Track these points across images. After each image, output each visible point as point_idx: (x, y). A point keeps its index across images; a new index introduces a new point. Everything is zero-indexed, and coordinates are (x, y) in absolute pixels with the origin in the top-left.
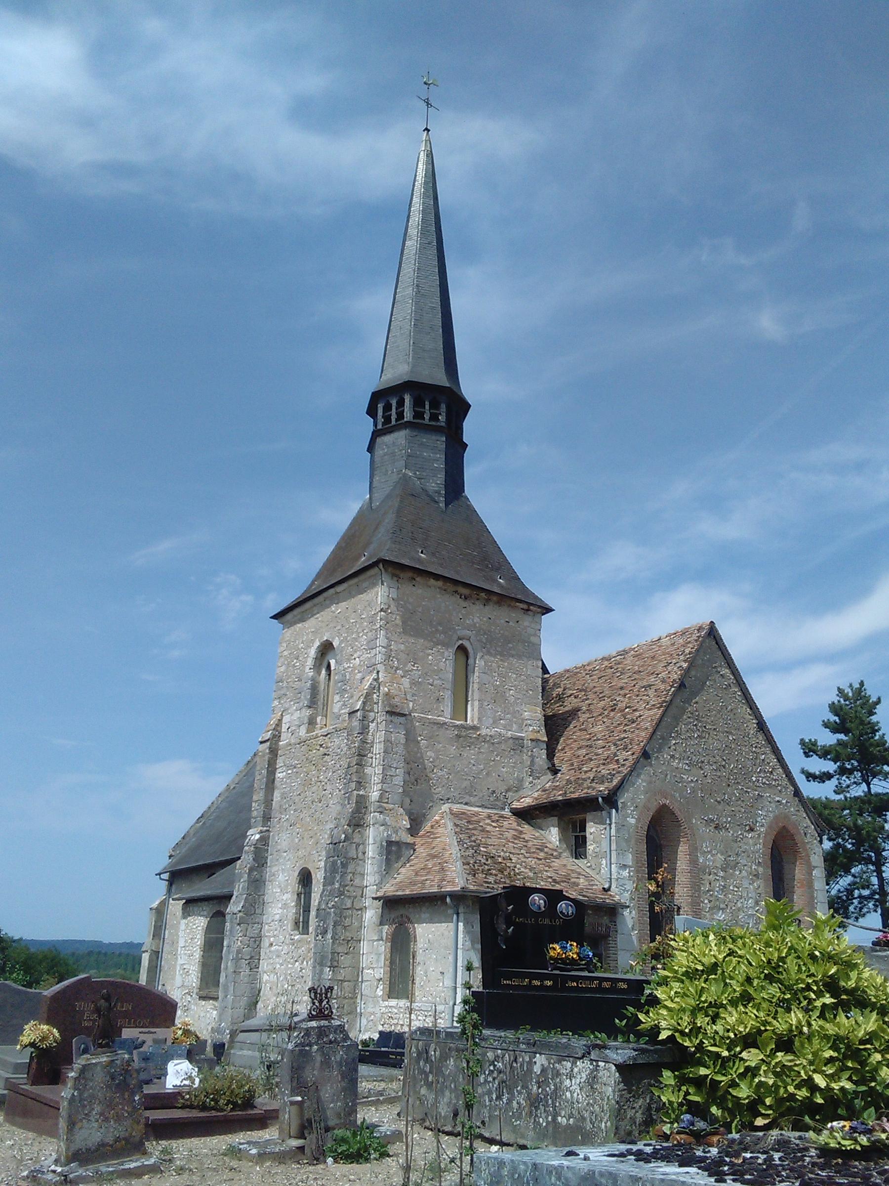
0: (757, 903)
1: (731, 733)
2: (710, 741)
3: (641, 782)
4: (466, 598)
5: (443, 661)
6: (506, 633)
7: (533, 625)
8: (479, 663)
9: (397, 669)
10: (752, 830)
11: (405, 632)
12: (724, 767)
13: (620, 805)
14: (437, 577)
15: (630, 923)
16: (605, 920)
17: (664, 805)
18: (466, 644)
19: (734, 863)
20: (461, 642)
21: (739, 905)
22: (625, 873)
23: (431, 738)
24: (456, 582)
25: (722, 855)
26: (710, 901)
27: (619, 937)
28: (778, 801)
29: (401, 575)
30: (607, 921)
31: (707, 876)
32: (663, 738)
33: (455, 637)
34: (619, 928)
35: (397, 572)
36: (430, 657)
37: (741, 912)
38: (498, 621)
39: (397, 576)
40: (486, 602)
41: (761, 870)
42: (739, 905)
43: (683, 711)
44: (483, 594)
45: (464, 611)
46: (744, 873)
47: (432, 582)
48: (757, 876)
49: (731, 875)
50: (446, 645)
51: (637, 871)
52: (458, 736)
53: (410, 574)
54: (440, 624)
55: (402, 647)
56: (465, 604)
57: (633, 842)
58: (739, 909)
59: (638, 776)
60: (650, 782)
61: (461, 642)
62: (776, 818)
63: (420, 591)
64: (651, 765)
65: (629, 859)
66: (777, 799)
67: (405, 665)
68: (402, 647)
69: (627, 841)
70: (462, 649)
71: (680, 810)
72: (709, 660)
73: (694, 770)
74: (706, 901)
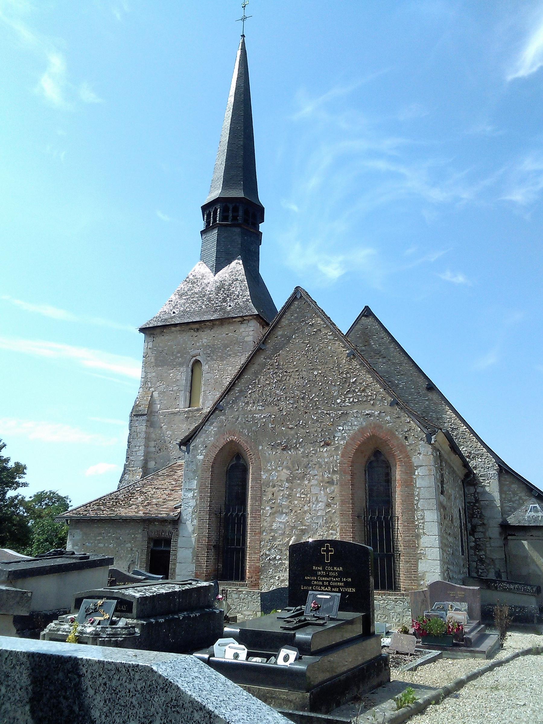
0: (328, 505)
1: (318, 369)
2: (292, 381)
3: (212, 429)
4: (198, 329)
5: (181, 375)
6: (226, 342)
7: (247, 330)
8: (205, 367)
9: (150, 388)
10: (327, 444)
11: (157, 365)
12: (303, 398)
13: (191, 447)
14: (175, 325)
15: (190, 528)
16: (169, 528)
17: (232, 441)
18: (198, 358)
19: (302, 474)
20: (194, 358)
21: (306, 508)
22: (190, 495)
23: (169, 423)
24: (188, 323)
25: (287, 470)
26: (272, 508)
27: (180, 540)
28: (367, 414)
29: (155, 333)
30: (171, 529)
31: (270, 489)
32: (241, 391)
33: (189, 357)
34: (181, 532)
35: (152, 332)
36: (171, 375)
37: (308, 514)
38: (220, 336)
39: (152, 334)
40: (211, 328)
41: (336, 477)
42: (306, 508)
43: (264, 365)
44: (208, 323)
45: (195, 339)
46: (314, 482)
47: (173, 329)
48: (331, 482)
49: (299, 484)
50: (181, 364)
51: (200, 492)
52: (187, 418)
53: (158, 330)
54: (178, 352)
55: (154, 374)
56: (196, 334)
57: (199, 472)
58: (305, 512)
59: (211, 424)
60: (221, 427)
61: (194, 358)
62: (362, 430)
63: (167, 337)
64: (224, 414)
65: (194, 484)
66: (367, 412)
67: (155, 384)
68: (154, 374)
69: (195, 472)
70: (197, 362)
71: (247, 442)
72: (296, 318)
73: (270, 409)
74: (268, 508)
